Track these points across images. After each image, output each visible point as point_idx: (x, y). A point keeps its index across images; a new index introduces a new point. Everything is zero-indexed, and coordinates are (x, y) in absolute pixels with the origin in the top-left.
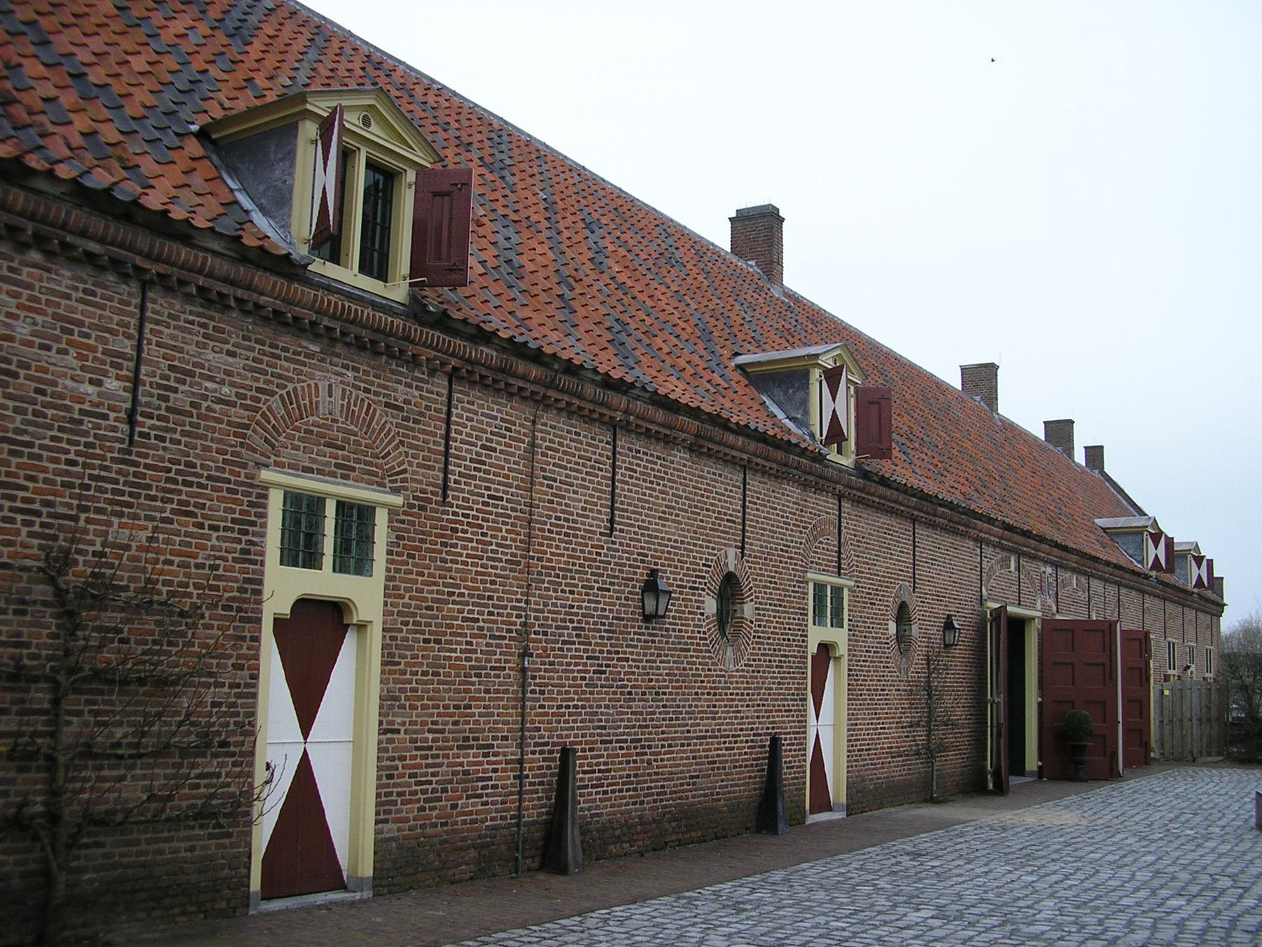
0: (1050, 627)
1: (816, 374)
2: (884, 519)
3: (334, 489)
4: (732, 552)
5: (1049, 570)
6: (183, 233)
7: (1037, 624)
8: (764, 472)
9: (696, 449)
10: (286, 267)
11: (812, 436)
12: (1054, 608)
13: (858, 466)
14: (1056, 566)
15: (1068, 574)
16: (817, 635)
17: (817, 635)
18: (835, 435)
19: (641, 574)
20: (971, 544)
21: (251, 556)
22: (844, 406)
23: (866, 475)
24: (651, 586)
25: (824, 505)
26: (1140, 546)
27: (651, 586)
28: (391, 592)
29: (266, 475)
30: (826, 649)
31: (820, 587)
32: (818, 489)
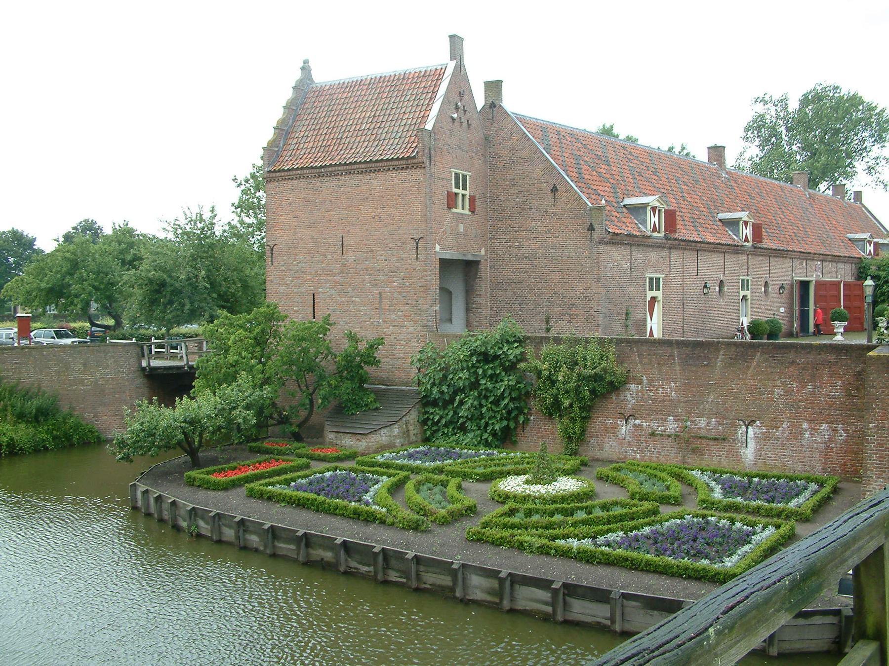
0: (819, 285)
1: (741, 222)
2: (761, 258)
4: (722, 275)
5: (819, 263)
6: (636, 236)
7: (814, 282)
8: (728, 252)
11: (741, 240)
12: (821, 276)
13: (753, 245)
14: (822, 261)
15: (827, 263)
16: (742, 293)
18: (746, 240)
19: (703, 284)
20: (789, 260)
21: (645, 290)
22: (748, 232)
23: (755, 248)
24: (705, 286)
25: (744, 258)
26: (864, 246)
27: (705, 286)
29: (647, 275)
31: (743, 280)
32: (742, 254)
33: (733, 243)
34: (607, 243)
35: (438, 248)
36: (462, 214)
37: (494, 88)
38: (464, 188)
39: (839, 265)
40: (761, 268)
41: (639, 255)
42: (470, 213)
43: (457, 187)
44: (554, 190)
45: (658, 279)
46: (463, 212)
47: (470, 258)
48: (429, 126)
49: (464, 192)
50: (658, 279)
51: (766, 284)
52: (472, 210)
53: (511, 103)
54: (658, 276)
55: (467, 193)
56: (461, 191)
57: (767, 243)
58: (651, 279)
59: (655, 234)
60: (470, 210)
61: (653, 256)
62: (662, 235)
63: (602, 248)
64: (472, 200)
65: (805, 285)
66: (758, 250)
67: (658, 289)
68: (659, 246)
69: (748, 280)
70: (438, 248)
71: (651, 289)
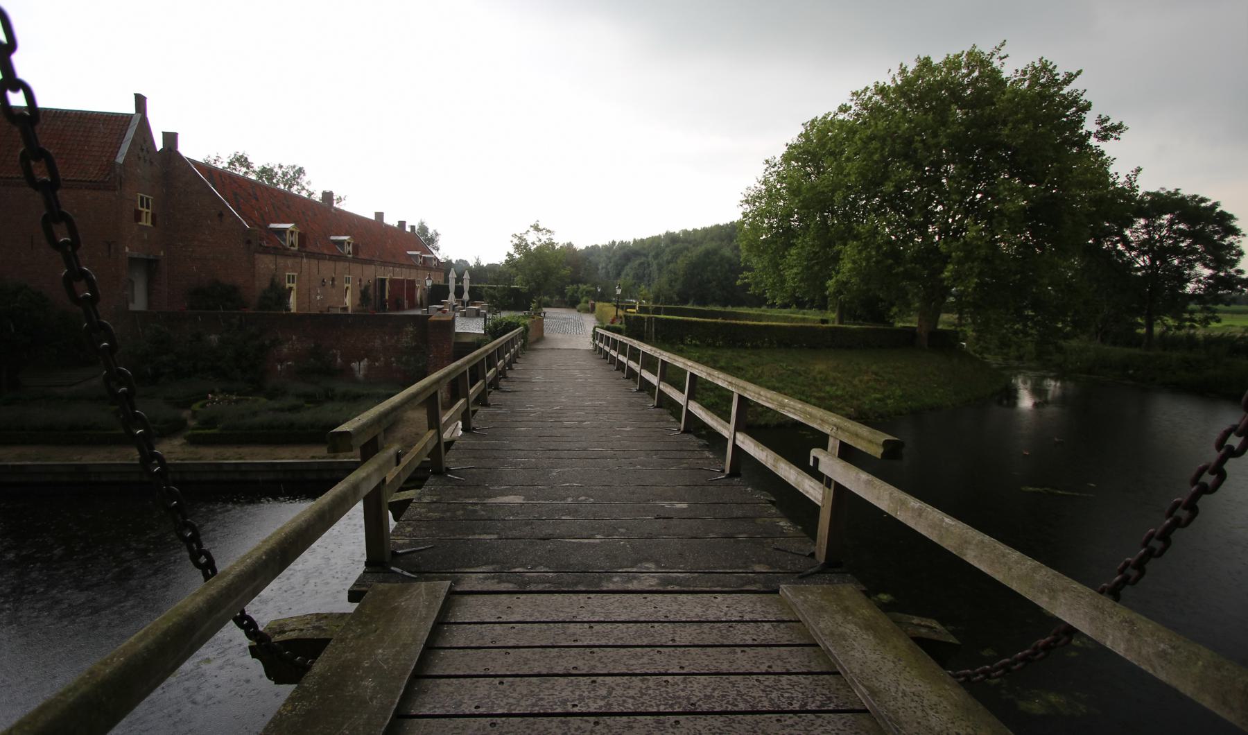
0: (392, 281)
3: (291, 274)
9: (329, 260)
10: (288, 249)
16: (346, 285)
17: (346, 285)
18: (349, 253)
22: (351, 248)
24: (323, 281)
25: (347, 264)
28: (297, 285)
30: (347, 288)
33: (338, 254)
34: (260, 253)
35: (127, 250)
36: (146, 226)
37: (170, 138)
38: (148, 208)
39: (404, 270)
40: (357, 269)
41: (281, 261)
42: (151, 226)
43: (142, 206)
44: (221, 215)
45: (293, 276)
46: (145, 224)
47: (151, 257)
48: (120, 159)
49: (147, 210)
50: (293, 276)
51: (360, 280)
52: (154, 222)
53: (187, 149)
54: (293, 274)
55: (150, 211)
56: (145, 210)
57: (361, 256)
58: (289, 276)
59: (292, 248)
60: (152, 224)
61: (290, 262)
62: (296, 248)
63: (257, 256)
64: (154, 217)
65: (383, 281)
66: (356, 259)
67: (293, 282)
68: (295, 255)
69: (349, 278)
70: (127, 250)
71: (289, 282)
